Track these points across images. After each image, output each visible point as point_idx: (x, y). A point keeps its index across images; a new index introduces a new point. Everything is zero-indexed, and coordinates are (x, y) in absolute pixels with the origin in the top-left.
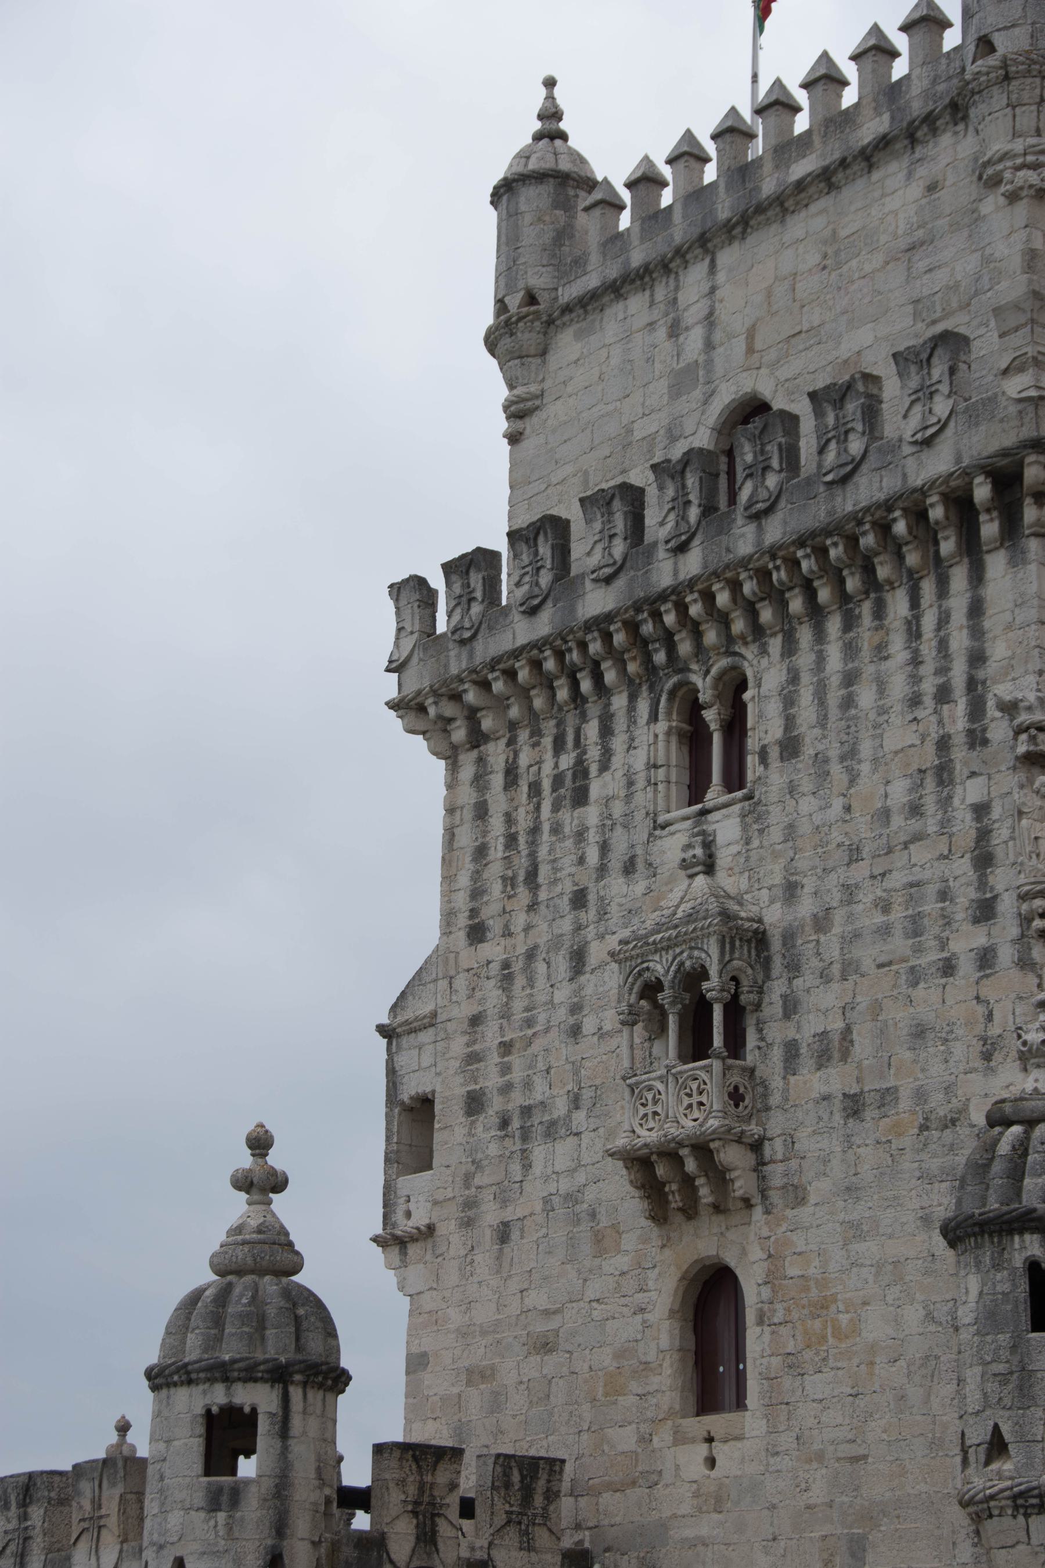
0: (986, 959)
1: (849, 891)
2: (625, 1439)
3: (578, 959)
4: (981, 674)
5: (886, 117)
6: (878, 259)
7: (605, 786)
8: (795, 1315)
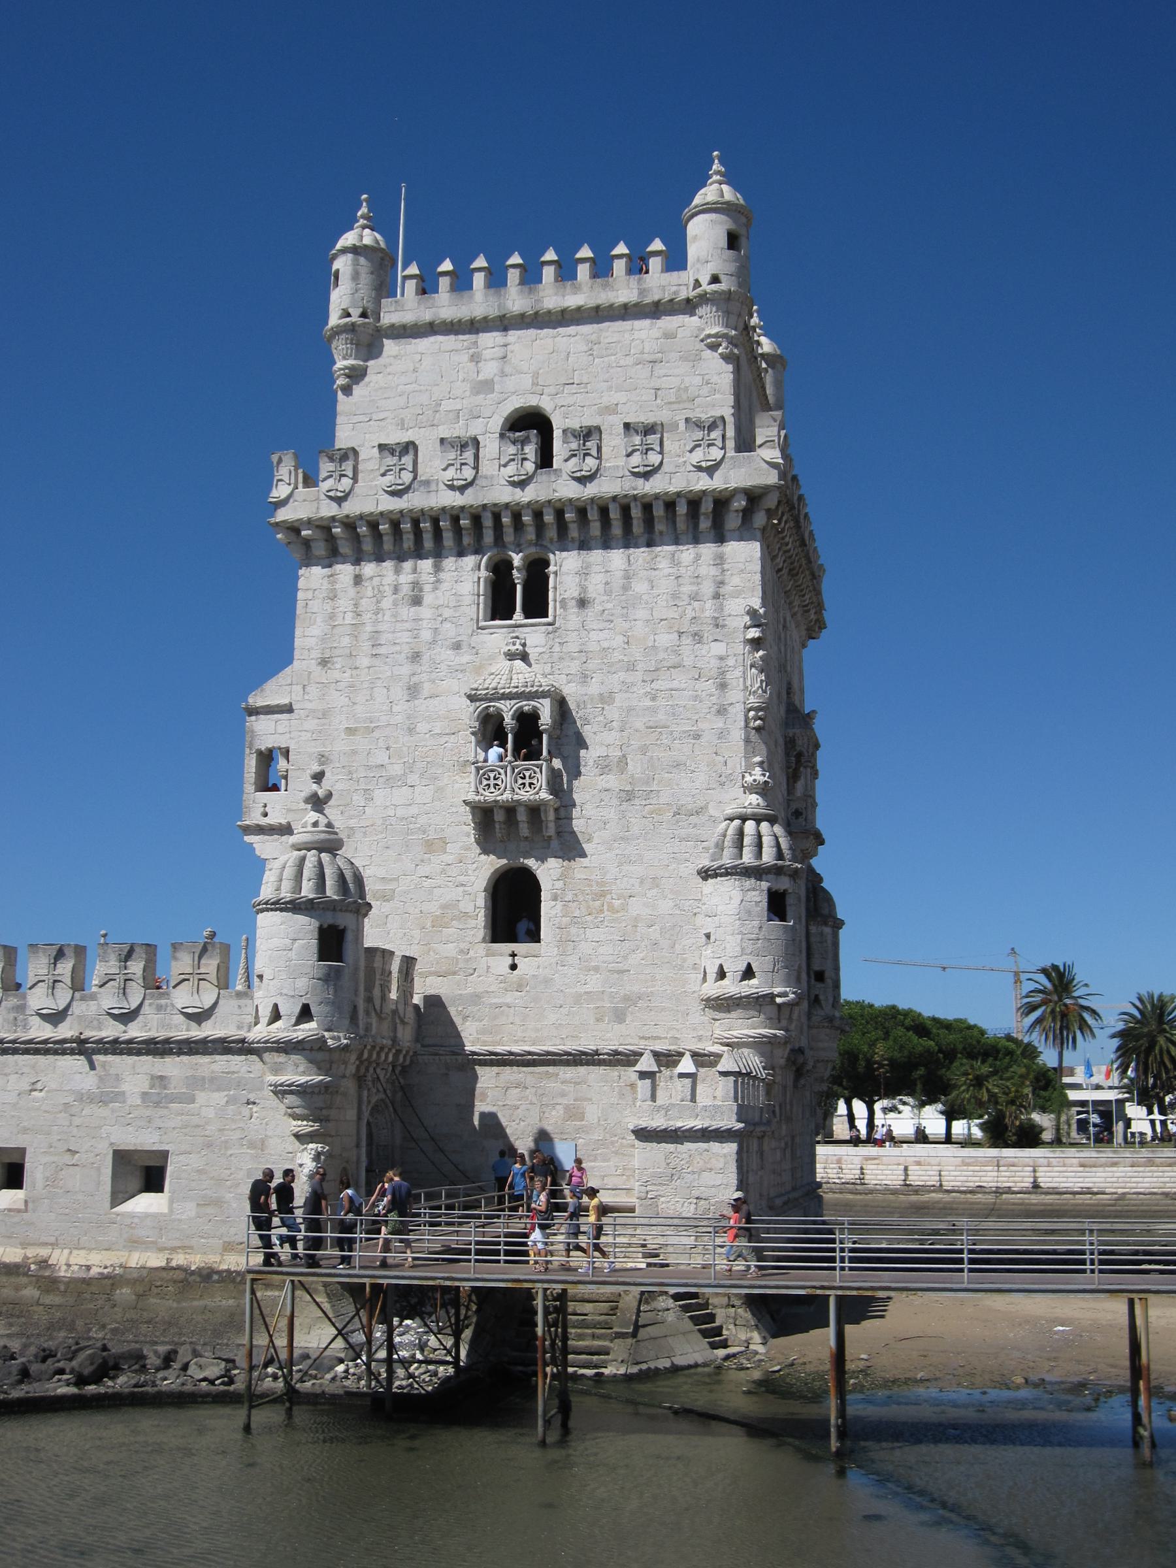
0: (722, 734)
1: (627, 687)
2: (450, 950)
3: (413, 691)
4: (722, 591)
5: (636, 292)
6: (630, 361)
7: (437, 598)
8: (581, 898)
